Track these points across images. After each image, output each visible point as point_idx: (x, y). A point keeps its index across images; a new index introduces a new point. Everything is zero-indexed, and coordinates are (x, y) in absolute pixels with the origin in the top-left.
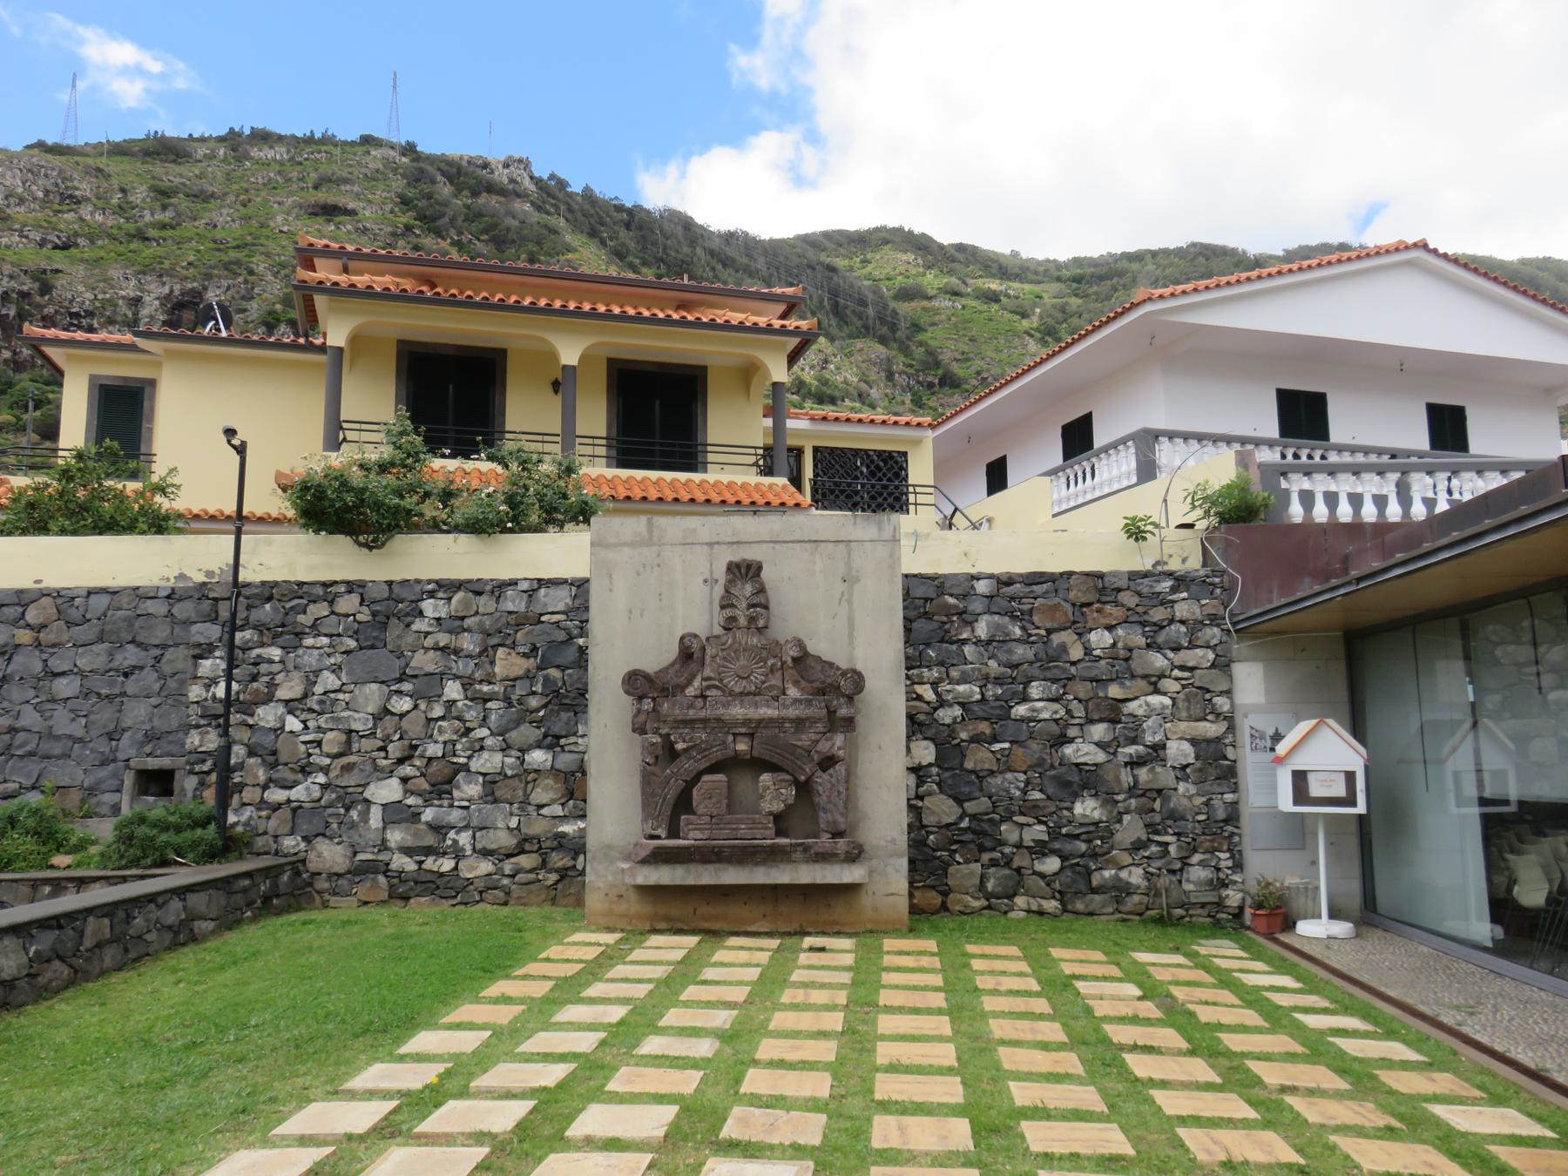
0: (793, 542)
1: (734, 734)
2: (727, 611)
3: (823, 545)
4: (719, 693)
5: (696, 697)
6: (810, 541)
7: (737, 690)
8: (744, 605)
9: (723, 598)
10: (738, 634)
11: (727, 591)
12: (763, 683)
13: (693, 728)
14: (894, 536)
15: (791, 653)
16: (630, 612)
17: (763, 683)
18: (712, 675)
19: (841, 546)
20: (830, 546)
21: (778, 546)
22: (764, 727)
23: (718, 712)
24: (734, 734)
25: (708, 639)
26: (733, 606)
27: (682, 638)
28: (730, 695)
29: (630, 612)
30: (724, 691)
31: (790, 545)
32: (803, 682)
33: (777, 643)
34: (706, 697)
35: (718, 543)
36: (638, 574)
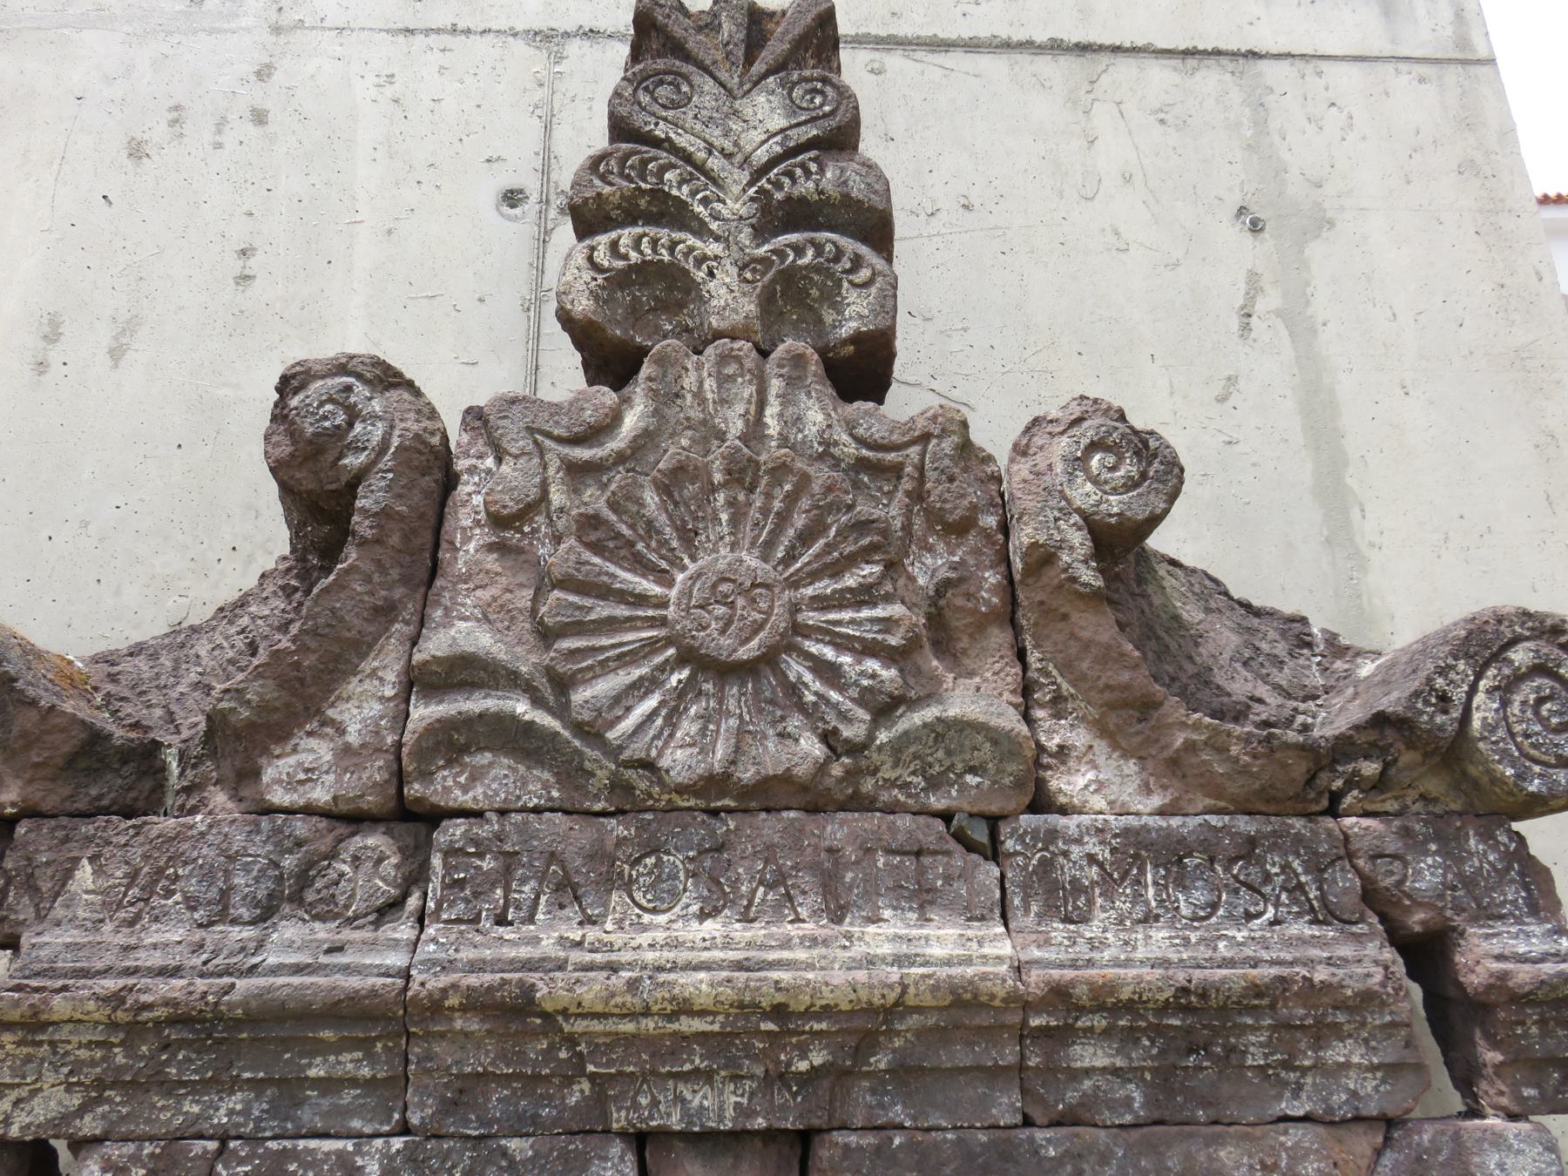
0: (972, 46)
1: (641, 1141)
2: (626, 236)
3: (1124, 68)
4: (538, 786)
5: (350, 818)
6: (1056, 47)
7: (679, 760)
8: (736, 204)
9: (595, 163)
10: (698, 375)
11: (620, 129)
12: (884, 707)
13: (289, 1090)
14: (1463, 42)
15: (1083, 493)
16: (52, 335)
17: (884, 707)
18: (483, 641)
19: (1210, 78)
20: (1160, 74)
21: (895, 61)
22: (905, 1074)
23: (511, 944)
24: (641, 1141)
25: (476, 418)
26: (670, 213)
27: (289, 384)
28: (625, 803)
29: (52, 335)
30: (572, 772)
31: (955, 59)
32: (1174, 709)
33: (966, 448)
34: (434, 817)
35: (592, 34)
36: (137, 151)
